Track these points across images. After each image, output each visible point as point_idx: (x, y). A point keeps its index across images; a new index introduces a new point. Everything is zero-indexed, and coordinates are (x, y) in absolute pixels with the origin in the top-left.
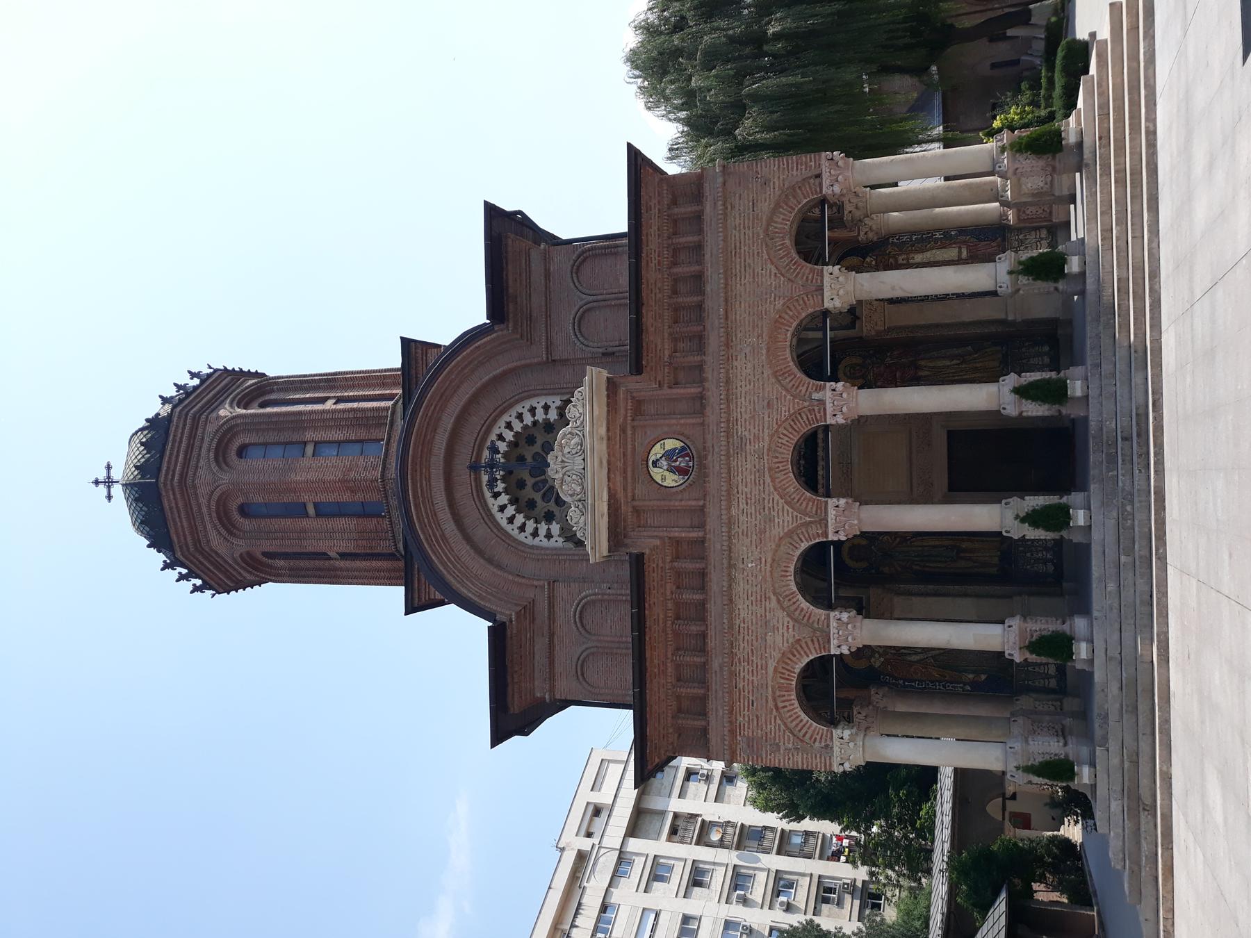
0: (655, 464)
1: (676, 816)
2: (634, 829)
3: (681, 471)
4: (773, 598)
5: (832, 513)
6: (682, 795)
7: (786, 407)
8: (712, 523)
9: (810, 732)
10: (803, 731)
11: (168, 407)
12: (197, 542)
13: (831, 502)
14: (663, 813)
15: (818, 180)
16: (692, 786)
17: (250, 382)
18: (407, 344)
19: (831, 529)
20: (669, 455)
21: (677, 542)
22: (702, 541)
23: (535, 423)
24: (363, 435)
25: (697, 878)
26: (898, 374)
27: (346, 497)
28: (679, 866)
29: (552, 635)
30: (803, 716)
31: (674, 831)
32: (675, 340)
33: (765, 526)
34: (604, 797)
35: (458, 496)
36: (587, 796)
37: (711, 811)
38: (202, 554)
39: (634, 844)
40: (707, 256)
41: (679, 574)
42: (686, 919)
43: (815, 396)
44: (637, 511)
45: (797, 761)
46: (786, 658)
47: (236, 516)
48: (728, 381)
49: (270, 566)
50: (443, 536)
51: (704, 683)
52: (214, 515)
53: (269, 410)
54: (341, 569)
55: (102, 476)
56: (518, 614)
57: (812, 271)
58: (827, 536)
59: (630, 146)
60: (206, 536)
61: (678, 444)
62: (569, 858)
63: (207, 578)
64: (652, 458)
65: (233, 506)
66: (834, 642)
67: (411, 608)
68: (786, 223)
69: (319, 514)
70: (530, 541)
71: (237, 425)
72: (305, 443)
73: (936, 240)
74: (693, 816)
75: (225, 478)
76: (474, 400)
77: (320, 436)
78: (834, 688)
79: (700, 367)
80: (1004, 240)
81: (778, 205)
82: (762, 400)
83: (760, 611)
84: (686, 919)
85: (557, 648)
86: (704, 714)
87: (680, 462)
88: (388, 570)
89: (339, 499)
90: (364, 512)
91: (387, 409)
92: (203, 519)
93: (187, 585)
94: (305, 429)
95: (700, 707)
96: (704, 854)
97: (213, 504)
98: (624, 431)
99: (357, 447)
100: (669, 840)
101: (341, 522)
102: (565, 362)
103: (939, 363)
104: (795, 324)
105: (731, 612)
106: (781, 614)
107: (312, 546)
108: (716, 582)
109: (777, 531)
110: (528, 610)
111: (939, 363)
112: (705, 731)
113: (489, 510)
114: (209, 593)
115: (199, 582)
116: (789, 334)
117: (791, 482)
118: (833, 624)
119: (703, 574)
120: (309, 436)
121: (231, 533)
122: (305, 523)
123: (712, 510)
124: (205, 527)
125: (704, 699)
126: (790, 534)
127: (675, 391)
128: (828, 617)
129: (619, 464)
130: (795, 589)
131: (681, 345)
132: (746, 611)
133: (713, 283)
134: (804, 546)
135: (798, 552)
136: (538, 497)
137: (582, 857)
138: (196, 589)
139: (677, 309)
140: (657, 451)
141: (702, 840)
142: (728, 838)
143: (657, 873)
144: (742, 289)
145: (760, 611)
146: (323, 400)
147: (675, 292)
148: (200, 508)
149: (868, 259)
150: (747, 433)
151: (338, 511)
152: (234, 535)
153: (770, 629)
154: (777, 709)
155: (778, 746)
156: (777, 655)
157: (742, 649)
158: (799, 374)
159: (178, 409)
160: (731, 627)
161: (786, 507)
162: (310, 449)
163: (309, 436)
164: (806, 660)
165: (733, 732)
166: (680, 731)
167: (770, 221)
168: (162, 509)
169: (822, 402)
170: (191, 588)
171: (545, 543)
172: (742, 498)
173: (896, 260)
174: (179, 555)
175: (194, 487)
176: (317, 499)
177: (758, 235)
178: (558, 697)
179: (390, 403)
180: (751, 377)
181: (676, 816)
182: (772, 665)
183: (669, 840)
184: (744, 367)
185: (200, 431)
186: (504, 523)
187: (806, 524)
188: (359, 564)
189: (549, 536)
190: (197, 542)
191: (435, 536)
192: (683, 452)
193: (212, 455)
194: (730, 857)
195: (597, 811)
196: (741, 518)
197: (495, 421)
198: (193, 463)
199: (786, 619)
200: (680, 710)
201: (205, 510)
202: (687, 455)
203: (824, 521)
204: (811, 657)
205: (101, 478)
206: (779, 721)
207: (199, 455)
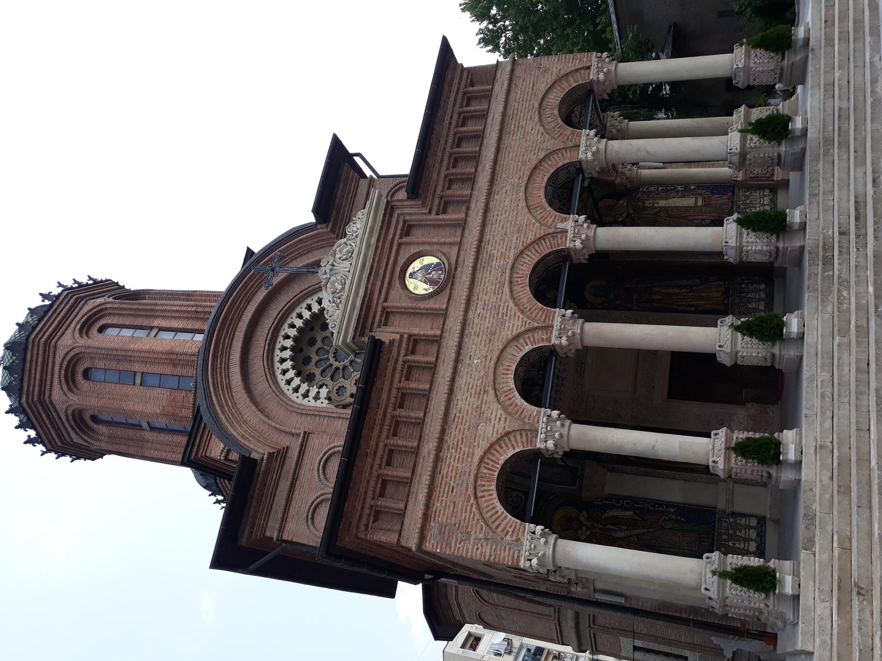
0: (412, 275)
4: (492, 392)
5: (558, 320)
9: (503, 524)
10: (497, 523)
11: (61, 289)
12: (41, 393)
15: (587, 71)
20: (426, 268)
26: (635, 296)
30: (499, 507)
38: (42, 405)
43: (560, 226)
47: (79, 377)
54: (148, 441)
57: (573, 133)
58: (550, 341)
59: (445, 39)
61: (435, 260)
63: (41, 431)
64: (410, 270)
65: (80, 369)
70: (300, 400)
71: (106, 309)
73: (678, 192)
80: (733, 195)
85: (296, 492)
87: (434, 275)
103: (671, 291)
104: (552, 171)
106: (496, 406)
109: (507, 334)
111: (671, 291)
113: (274, 372)
114: (40, 448)
115: (32, 433)
116: (546, 179)
117: (525, 293)
127: (441, 217)
128: (540, 412)
130: (513, 386)
135: (522, 354)
138: (30, 441)
140: (416, 265)
144: (513, 143)
145: (477, 403)
149: (621, 202)
150: (495, 252)
154: (476, 497)
155: (469, 533)
158: (549, 208)
161: (518, 313)
164: (511, 452)
168: (24, 360)
170: (26, 439)
172: (481, 304)
173: (644, 203)
174: (24, 400)
175: (55, 347)
177: (533, 106)
178: (285, 537)
180: (508, 208)
186: (282, 384)
190: (41, 393)
191: (222, 382)
193: (79, 326)
196: (476, 321)
199: (500, 412)
202: (441, 269)
203: (549, 328)
204: (517, 450)
206: (474, 509)
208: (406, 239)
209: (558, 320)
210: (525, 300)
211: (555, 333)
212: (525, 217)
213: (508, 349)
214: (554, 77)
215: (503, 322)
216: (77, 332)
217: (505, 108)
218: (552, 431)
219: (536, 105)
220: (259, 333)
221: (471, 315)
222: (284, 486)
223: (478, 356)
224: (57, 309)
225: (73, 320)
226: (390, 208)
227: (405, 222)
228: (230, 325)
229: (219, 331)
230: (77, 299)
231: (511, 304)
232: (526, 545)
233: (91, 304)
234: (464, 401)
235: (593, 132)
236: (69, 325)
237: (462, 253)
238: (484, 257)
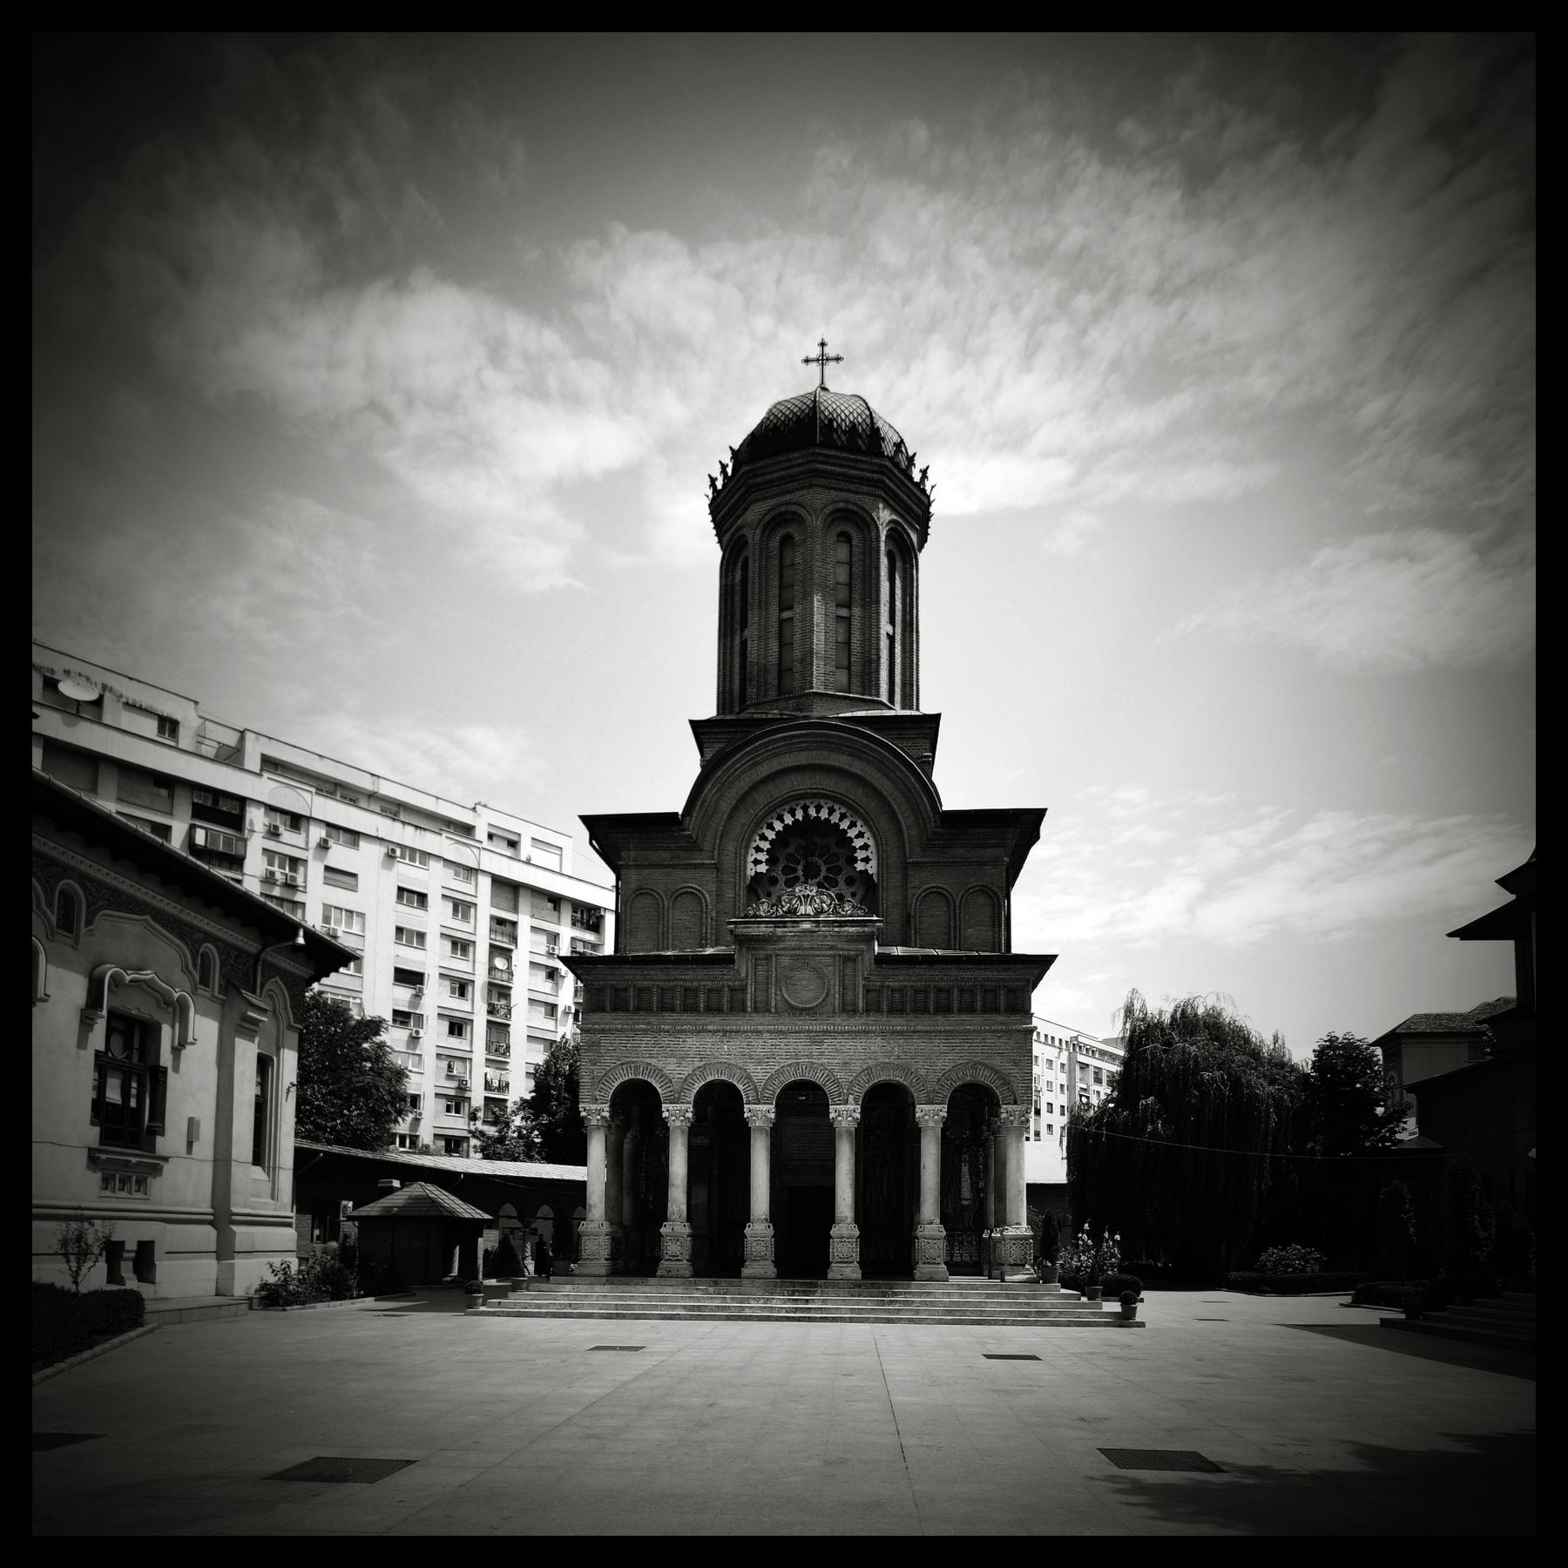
1: (514, 924)
2: (499, 882)
5: (764, 1107)
6: (534, 929)
8: (758, 1018)
14: (515, 910)
16: (543, 939)
17: (914, 537)
18: (936, 719)
19: (752, 1107)
21: (743, 990)
22: (744, 1011)
23: (855, 849)
24: (855, 669)
25: (461, 946)
27: (797, 653)
28: (467, 927)
29: (673, 866)
30: (616, 1084)
31: (500, 922)
32: (901, 990)
33: (757, 1058)
34: (526, 849)
36: (526, 834)
37: (521, 957)
39: (485, 883)
40: (964, 1017)
41: (719, 991)
42: (421, 936)
44: (768, 958)
45: (585, 1079)
46: (658, 1072)
48: (866, 1032)
49: (735, 565)
50: (757, 764)
51: (638, 1009)
52: (783, 509)
53: (884, 561)
55: (830, 351)
56: (690, 836)
60: (764, 499)
62: (465, 817)
66: (670, 1107)
67: (696, 726)
68: (984, 1077)
69: (782, 622)
72: (849, 607)
74: (514, 939)
75: (817, 522)
76: (877, 793)
77: (856, 622)
78: (637, 1106)
79: (879, 1010)
81: (997, 1072)
82: (847, 1060)
83: (692, 1054)
84: (421, 936)
86: (615, 1009)
88: (731, 690)
89: (796, 646)
90: (783, 670)
91: (878, 695)
92: (780, 495)
93: (717, 473)
94: (863, 606)
95: (619, 1007)
96: (482, 951)
97: (793, 508)
98: (831, 948)
99: (845, 662)
100: (493, 918)
101: (774, 646)
102: (905, 880)
105: (691, 1032)
106: (689, 1070)
107: (753, 617)
108: (713, 1023)
109: (751, 1068)
110: (694, 846)
112: (603, 1010)
118: (684, 1107)
119: (719, 1011)
120: (857, 611)
121: (765, 527)
122: (774, 609)
123: (768, 1018)
124: (771, 497)
125: (626, 1010)
126: (749, 1077)
129: (806, 944)
131: (897, 995)
132: (692, 1043)
133: (943, 1023)
134: (740, 1087)
137: (468, 830)
138: (713, 481)
139: (925, 991)
141: (495, 950)
142: (498, 975)
143: (462, 907)
145: (692, 1054)
146: (892, 622)
147: (940, 990)
148: (789, 492)
151: (784, 645)
152: (764, 531)
153: (681, 1061)
156: (660, 1065)
157: (666, 1040)
159: (888, 464)
160: (681, 1032)
162: (844, 612)
163: (857, 611)
165: (603, 1031)
166: (601, 990)
167: (986, 1066)
169: (846, 1102)
171: (750, 859)
176: (797, 623)
179: (884, 698)
181: (514, 924)
182: (653, 1061)
183: (493, 918)
184: (876, 1045)
185: (866, 489)
187: (755, 1089)
188: (737, 661)
189: (757, 862)
194: (481, 978)
195: (513, 844)
198: (833, 483)
200: (617, 990)
201: (787, 498)
205: (827, 350)
207: (841, 490)
212: (857, 1067)
218: (678, 1114)
222: (664, 856)
225: (849, 491)
232: (594, 1107)
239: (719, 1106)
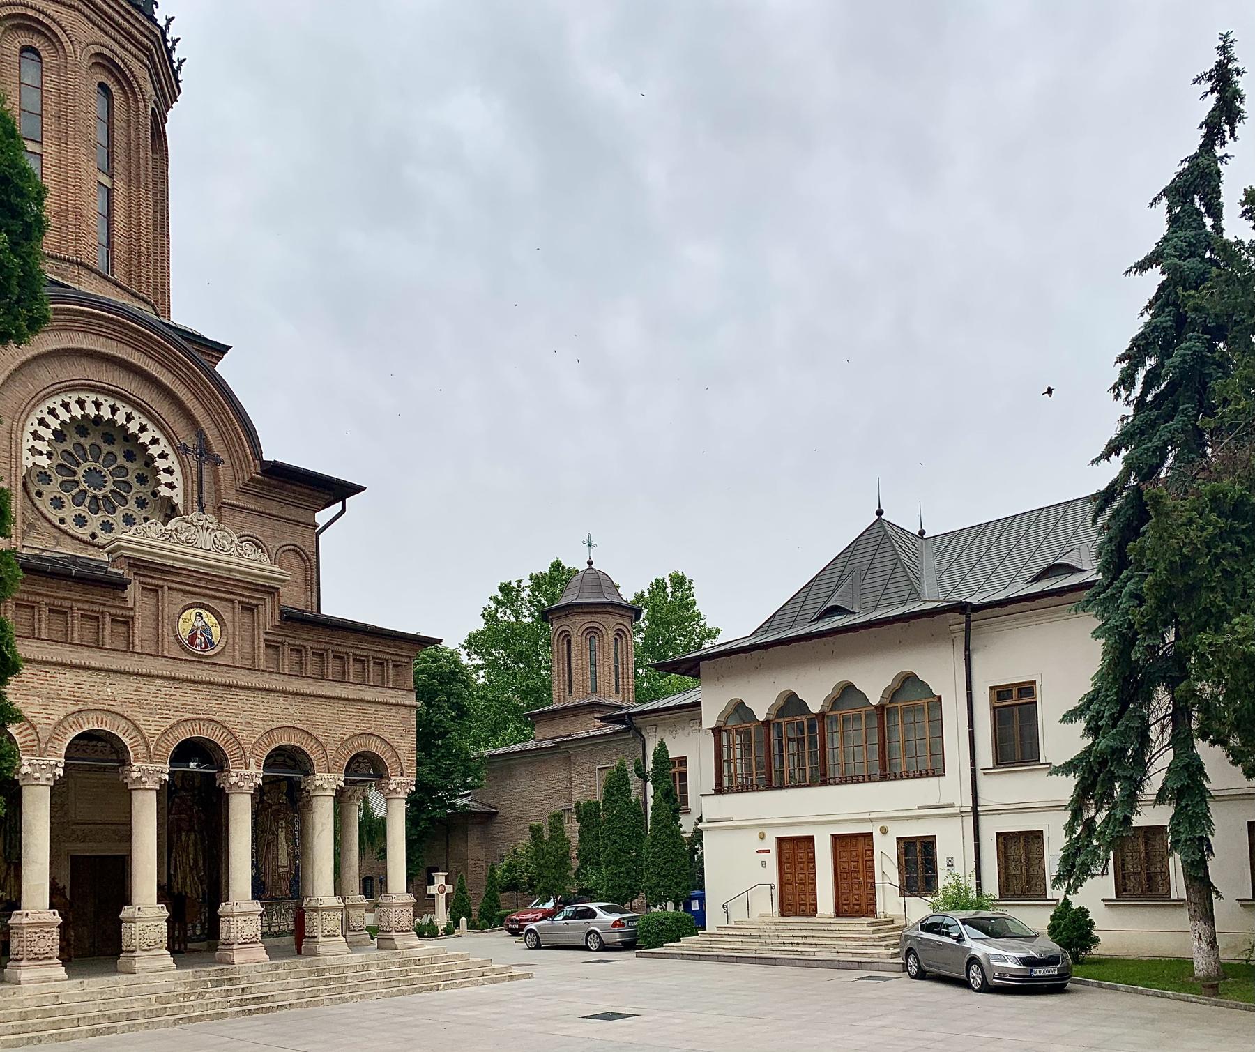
3: (192, 639)
5: (158, 767)
7: (247, 739)
13: (167, 767)
20: (206, 629)
35: (84, 361)
61: (215, 640)
83: (64, 694)
87: (200, 640)
109: (140, 719)
117: (184, 734)
127: (262, 644)
134: (126, 741)
135: (120, 736)
136: (68, 446)
140: (210, 619)
163: (120, 186)
186: (50, 403)
192: (209, 643)
193: (107, 52)
197: (162, 429)
208: (237, 605)
209: (158, 767)
210: (176, 734)
211: (144, 766)
213: (124, 721)
214: (395, 745)
215: (151, 715)
216: (97, 49)
217: (369, 702)
219: (370, 731)
220: (116, 373)
221: (159, 682)
223: (117, 691)
224: (132, 15)
226: (272, 591)
227: (257, 606)
228: (126, 335)
229: (118, 321)
230: (150, 51)
231: (172, 722)
233: (142, 74)
234: (65, 679)
235: (342, 783)
236: (107, 34)
237: (225, 669)
238: (220, 691)
239: (97, 759)
